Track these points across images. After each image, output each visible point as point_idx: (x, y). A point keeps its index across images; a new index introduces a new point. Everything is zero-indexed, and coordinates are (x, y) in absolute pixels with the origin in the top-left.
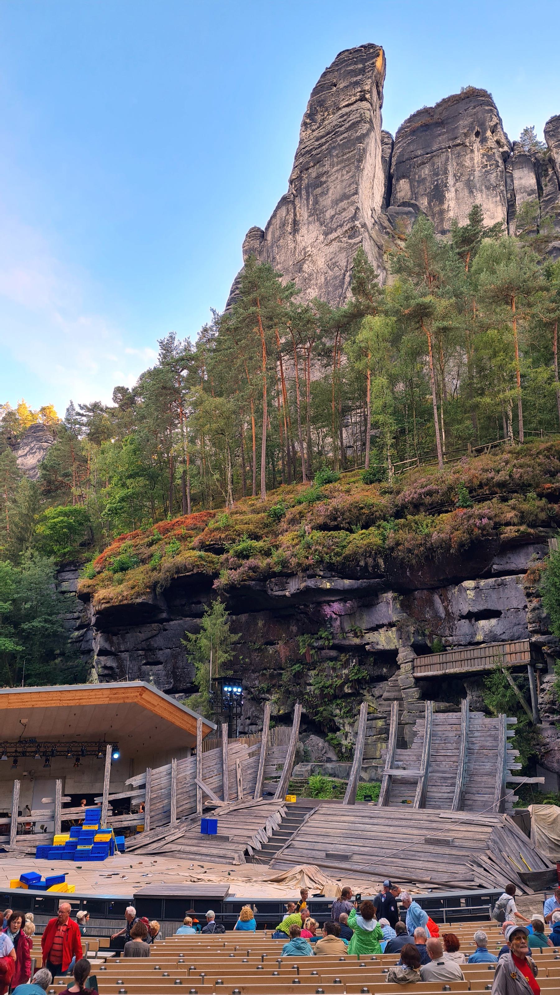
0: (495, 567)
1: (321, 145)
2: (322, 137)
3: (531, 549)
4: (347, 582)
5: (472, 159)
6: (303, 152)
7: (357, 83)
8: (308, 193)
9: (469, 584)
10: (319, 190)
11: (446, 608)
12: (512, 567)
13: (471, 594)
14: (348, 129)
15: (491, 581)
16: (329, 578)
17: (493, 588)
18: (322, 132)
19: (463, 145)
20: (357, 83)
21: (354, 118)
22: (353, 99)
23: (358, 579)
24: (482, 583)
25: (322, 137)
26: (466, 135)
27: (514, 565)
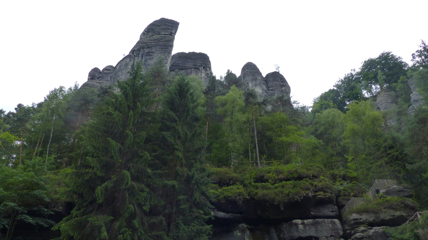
0: (312, 213)
1: (151, 43)
2: (152, 40)
3: (330, 205)
4: (221, 214)
5: (201, 75)
6: (142, 42)
7: (169, 29)
8: (142, 57)
9: (299, 221)
10: (148, 57)
11: (278, 236)
12: (321, 214)
13: (301, 227)
14: (164, 41)
15: (310, 221)
16: (213, 210)
17: (312, 224)
18: (152, 39)
19: (198, 69)
20: (169, 29)
21: (167, 39)
22: (167, 33)
23: (228, 213)
24: (306, 221)
25: (152, 40)
26: (200, 66)
27: (322, 213)
